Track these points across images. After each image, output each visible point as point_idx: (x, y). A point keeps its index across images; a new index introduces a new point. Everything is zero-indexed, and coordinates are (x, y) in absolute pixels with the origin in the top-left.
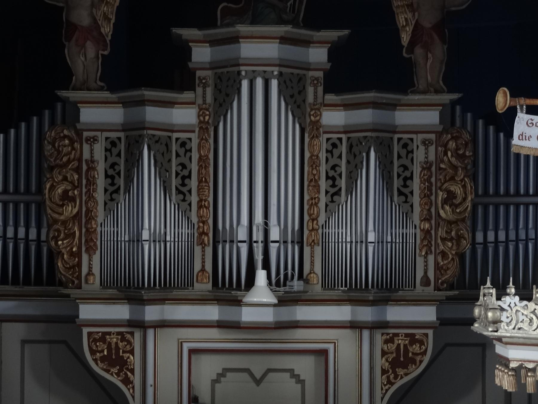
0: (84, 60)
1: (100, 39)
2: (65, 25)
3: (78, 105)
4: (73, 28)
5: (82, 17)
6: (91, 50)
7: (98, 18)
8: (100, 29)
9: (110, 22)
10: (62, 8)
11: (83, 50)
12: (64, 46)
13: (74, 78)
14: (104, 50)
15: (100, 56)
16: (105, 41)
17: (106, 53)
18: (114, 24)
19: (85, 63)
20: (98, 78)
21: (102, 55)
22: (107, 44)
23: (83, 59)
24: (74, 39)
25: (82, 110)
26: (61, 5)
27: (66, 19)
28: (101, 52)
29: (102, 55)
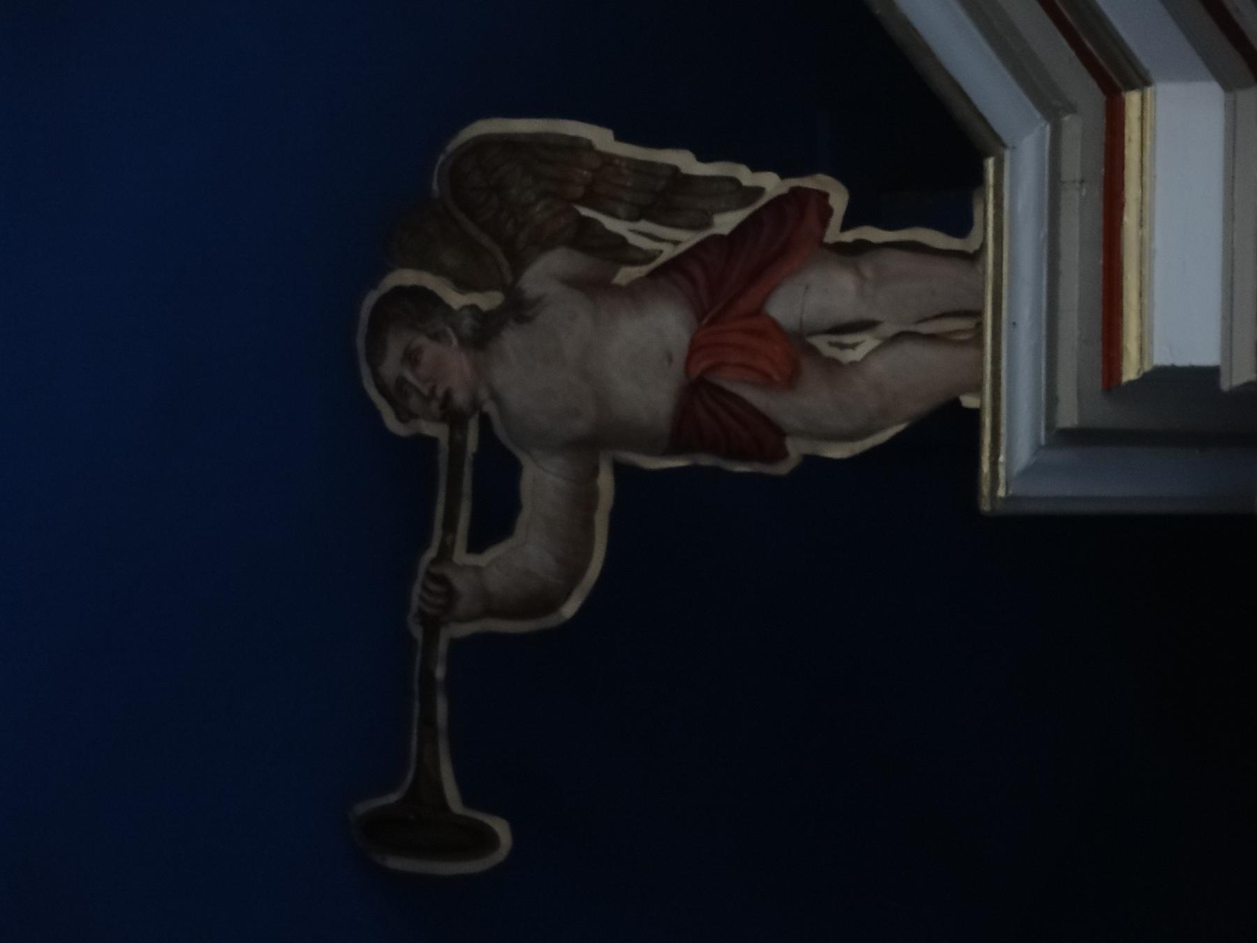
0: (856, 333)
1: (779, 238)
2: (706, 460)
3: (1130, 373)
4: (704, 411)
5: (639, 352)
6: (811, 296)
7: (668, 252)
8: (718, 238)
9: (690, 179)
10: (624, 474)
11: (821, 343)
12: (812, 462)
13: (969, 401)
14: (827, 212)
15: (849, 236)
16: (778, 201)
17: (839, 200)
18: (703, 157)
19: (889, 329)
20: (955, 244)
21: (845, 226)
22: (795, 191)
23: (868, 342)
24: (755, 397)
25: (1162, 357)
26: (605, 481)
27: (674, 449)
28: (834, 234)
29: (845, 226)
